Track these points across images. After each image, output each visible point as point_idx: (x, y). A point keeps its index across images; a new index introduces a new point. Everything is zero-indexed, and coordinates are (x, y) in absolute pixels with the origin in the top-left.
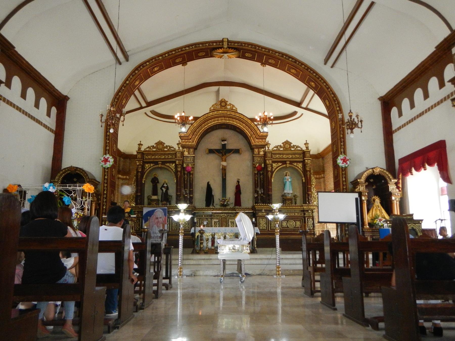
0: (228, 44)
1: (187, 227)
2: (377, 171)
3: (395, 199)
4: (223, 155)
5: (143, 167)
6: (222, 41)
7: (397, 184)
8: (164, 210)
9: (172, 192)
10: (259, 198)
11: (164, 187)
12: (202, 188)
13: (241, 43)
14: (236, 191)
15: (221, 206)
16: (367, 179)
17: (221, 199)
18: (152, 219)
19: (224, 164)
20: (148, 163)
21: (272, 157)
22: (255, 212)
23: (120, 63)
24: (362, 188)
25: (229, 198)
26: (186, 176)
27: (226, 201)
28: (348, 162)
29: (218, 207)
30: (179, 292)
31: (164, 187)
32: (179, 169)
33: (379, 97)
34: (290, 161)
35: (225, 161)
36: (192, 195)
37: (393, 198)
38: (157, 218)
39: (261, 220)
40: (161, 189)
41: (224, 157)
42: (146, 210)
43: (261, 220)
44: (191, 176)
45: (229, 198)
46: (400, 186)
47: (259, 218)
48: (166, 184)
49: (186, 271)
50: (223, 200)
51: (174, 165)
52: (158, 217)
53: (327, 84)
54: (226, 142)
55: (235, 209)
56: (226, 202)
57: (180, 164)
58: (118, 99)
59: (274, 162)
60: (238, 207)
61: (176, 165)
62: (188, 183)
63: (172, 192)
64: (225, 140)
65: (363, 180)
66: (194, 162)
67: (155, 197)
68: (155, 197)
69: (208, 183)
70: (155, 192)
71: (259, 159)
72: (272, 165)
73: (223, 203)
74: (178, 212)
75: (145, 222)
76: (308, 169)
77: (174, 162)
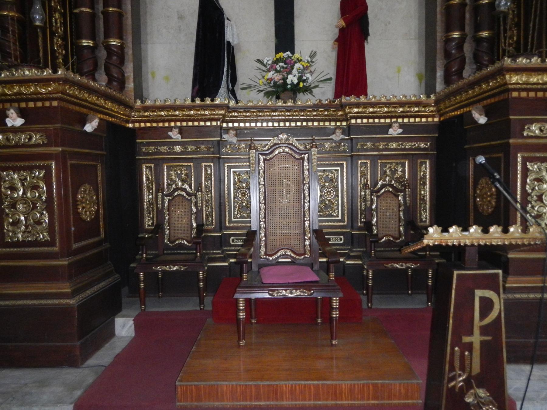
1: (39, 222)
10: (468, 49)
12: (181, 17)
14: (344, 20)
15: (268, 94)
17: (269, 59)
22: (482, 120)
25: (313, 55)
27: (297, 66)
29: (260, 100)
36: (120, 37)
45: (313, 55)
47: (525, 160)
50: (276, 62)
55: (342, 107)
56: (295, 71)
60: (363, 99)
73: (277, 77)
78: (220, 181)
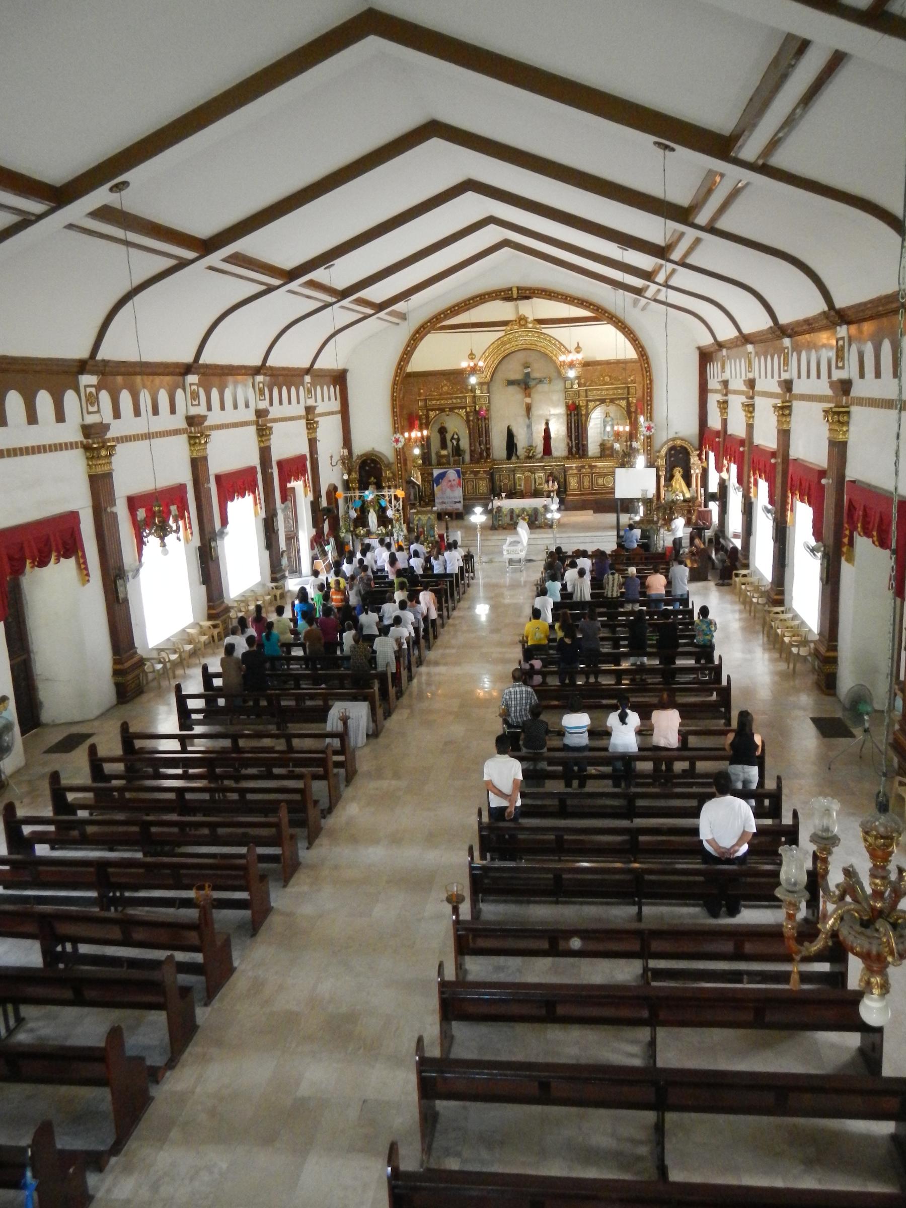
0: (518, 293)
2: (679, 442)
3: (696, 471)
4: (526, 389)
5: (427, 417)
6: (511, 289)
7: (700, 456)
8: (458, 472)
9: (465, 444)
11: (454, 439)
13: (534, 290)
16: (672, 448)
18: (444, 483)
19: (528, 400)
20: (432, 410)
21: (587, 397)
23: (398, 324)
24: (661, 462)
25: (536, 447)
26: (480, 421)
28: (653, 430)
30: (481, 581)
31: (454, 439)
32: (471, 418)
33: (697, 346)
34: (610, 399)
35: (529, 396)
37: (692, 472)
38: (450, 481)
39: (571, 478)
40: (451, 441)
41: (527, 391)
42: (436, 472)
43: (571, 478)
44: (487, 421)
46: (704, 457)
48: (457, 434)
49: (485, 559)
51: (464, 410)
52: (451, 478)
53: (634, 336)
54: (529, 370)
57: (471, 412)
58: (401, 370)
59: (591, 401)
61: (466, 412)
62: (484, 432)
63: (465, 444)
64: (529, 367)
65: (664, 451)
66: (489, 403)
67: (444, 452)
68: (444, 452)
69: (508, 427)
70: (444, 445)
71: (571, 395)
72: (587, 405)
74: (476, 514)
75: (437, 486)
76: (632, 409)
77: (465, 408)
78: (514, 478)
